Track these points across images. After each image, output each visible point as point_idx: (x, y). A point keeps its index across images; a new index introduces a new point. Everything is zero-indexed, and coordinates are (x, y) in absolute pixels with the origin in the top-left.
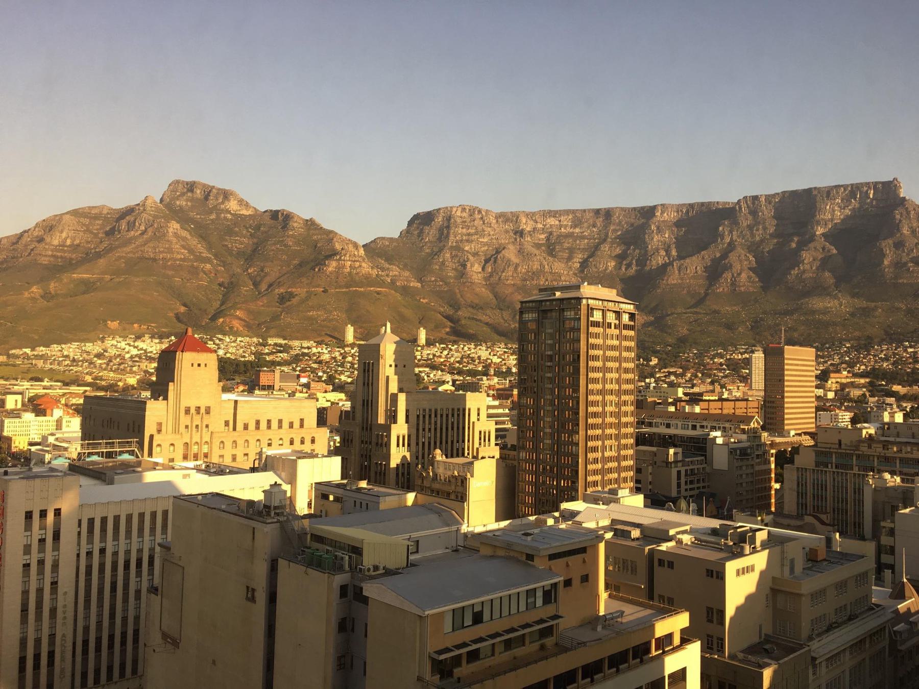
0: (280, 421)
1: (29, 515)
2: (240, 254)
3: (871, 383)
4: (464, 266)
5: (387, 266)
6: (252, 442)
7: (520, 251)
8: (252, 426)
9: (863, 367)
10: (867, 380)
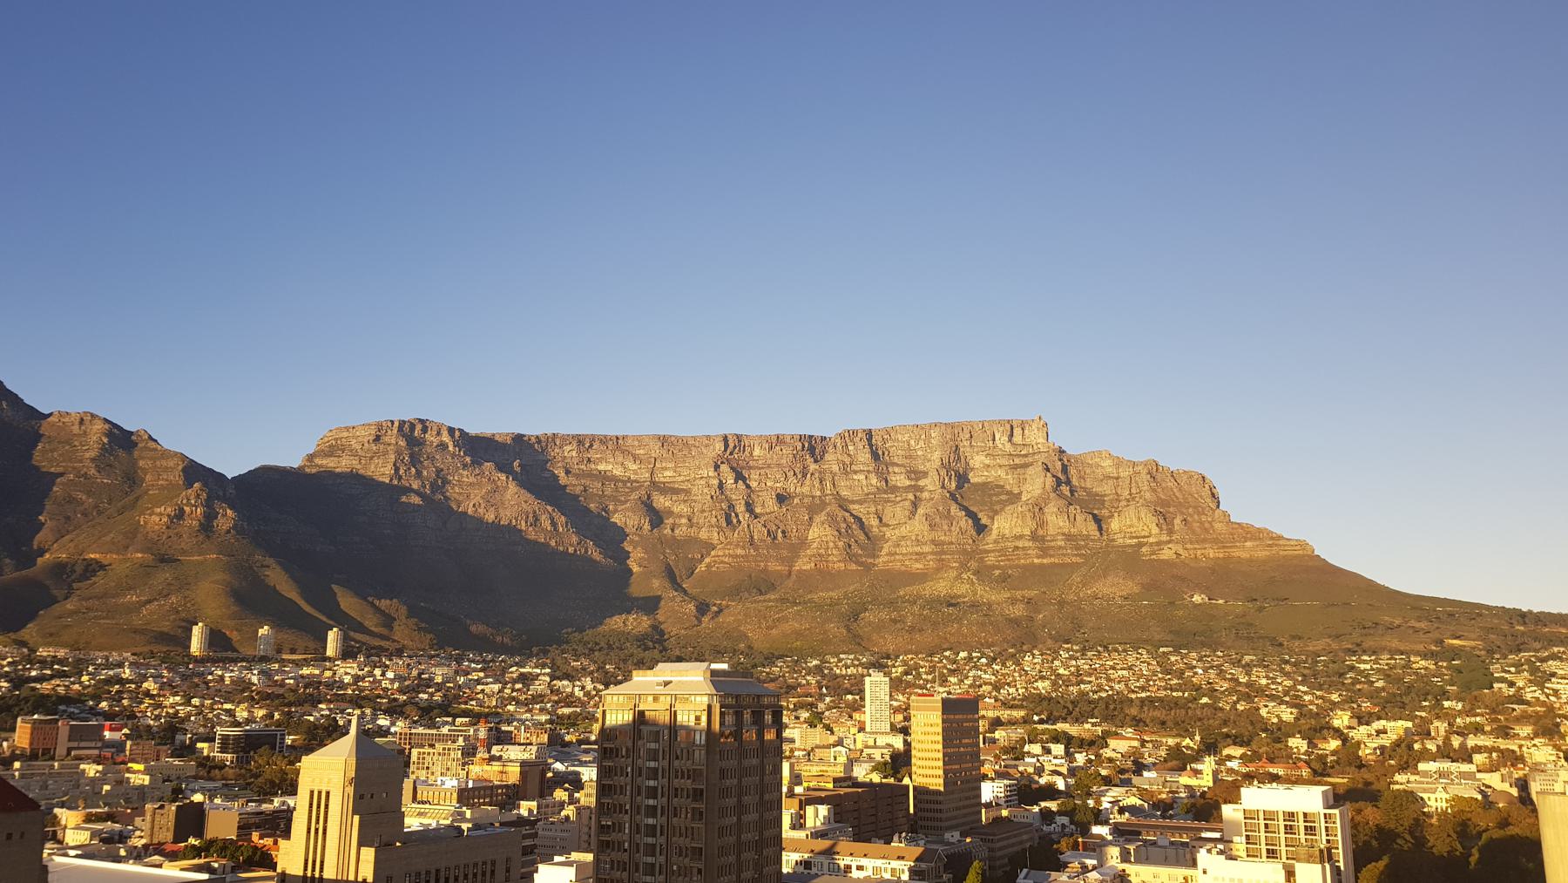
3: (1026, 721)
9: (1012, 690)
10: (1022, 713)
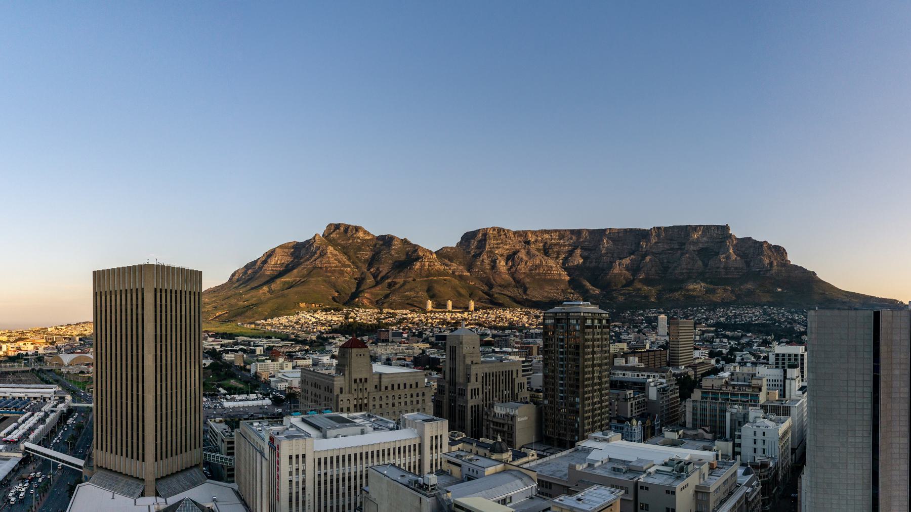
0: (405, 385)
1: (291, 457)
2: (365, 261)
4: (494, 261)
5: (449, 263)
6: (390, 397)
7: (528, 253)
8: (390, 388)
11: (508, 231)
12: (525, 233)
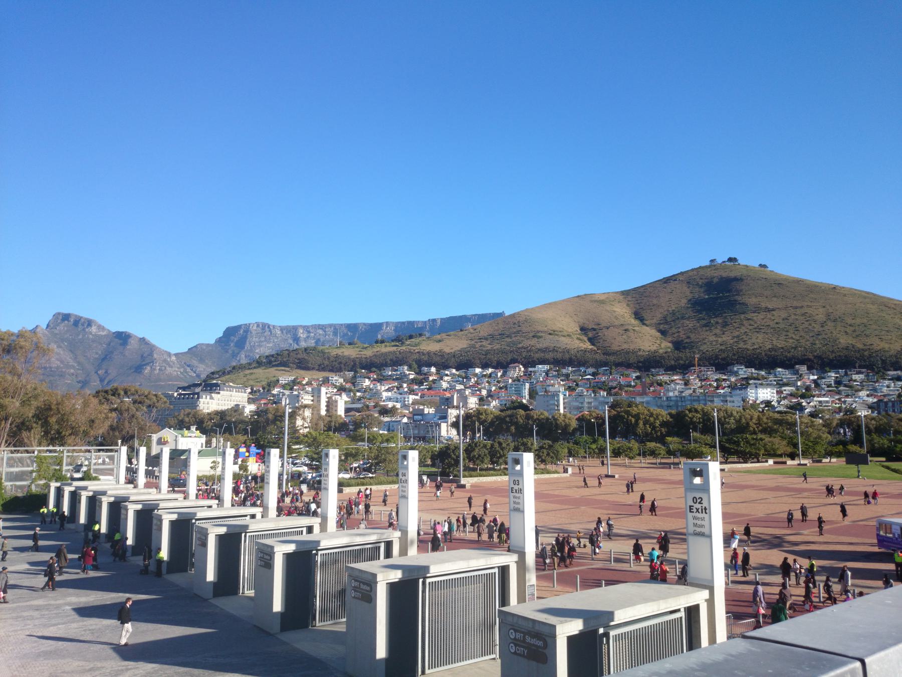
11: (274, 327)
12: (295, 328)
